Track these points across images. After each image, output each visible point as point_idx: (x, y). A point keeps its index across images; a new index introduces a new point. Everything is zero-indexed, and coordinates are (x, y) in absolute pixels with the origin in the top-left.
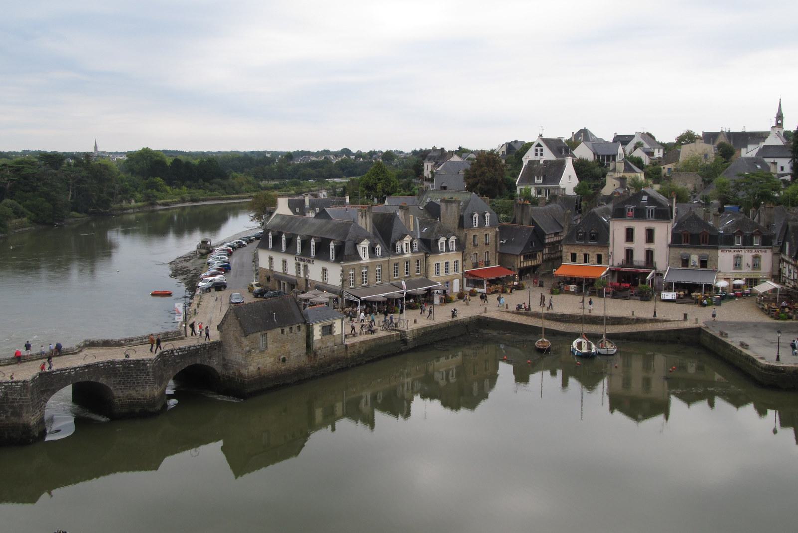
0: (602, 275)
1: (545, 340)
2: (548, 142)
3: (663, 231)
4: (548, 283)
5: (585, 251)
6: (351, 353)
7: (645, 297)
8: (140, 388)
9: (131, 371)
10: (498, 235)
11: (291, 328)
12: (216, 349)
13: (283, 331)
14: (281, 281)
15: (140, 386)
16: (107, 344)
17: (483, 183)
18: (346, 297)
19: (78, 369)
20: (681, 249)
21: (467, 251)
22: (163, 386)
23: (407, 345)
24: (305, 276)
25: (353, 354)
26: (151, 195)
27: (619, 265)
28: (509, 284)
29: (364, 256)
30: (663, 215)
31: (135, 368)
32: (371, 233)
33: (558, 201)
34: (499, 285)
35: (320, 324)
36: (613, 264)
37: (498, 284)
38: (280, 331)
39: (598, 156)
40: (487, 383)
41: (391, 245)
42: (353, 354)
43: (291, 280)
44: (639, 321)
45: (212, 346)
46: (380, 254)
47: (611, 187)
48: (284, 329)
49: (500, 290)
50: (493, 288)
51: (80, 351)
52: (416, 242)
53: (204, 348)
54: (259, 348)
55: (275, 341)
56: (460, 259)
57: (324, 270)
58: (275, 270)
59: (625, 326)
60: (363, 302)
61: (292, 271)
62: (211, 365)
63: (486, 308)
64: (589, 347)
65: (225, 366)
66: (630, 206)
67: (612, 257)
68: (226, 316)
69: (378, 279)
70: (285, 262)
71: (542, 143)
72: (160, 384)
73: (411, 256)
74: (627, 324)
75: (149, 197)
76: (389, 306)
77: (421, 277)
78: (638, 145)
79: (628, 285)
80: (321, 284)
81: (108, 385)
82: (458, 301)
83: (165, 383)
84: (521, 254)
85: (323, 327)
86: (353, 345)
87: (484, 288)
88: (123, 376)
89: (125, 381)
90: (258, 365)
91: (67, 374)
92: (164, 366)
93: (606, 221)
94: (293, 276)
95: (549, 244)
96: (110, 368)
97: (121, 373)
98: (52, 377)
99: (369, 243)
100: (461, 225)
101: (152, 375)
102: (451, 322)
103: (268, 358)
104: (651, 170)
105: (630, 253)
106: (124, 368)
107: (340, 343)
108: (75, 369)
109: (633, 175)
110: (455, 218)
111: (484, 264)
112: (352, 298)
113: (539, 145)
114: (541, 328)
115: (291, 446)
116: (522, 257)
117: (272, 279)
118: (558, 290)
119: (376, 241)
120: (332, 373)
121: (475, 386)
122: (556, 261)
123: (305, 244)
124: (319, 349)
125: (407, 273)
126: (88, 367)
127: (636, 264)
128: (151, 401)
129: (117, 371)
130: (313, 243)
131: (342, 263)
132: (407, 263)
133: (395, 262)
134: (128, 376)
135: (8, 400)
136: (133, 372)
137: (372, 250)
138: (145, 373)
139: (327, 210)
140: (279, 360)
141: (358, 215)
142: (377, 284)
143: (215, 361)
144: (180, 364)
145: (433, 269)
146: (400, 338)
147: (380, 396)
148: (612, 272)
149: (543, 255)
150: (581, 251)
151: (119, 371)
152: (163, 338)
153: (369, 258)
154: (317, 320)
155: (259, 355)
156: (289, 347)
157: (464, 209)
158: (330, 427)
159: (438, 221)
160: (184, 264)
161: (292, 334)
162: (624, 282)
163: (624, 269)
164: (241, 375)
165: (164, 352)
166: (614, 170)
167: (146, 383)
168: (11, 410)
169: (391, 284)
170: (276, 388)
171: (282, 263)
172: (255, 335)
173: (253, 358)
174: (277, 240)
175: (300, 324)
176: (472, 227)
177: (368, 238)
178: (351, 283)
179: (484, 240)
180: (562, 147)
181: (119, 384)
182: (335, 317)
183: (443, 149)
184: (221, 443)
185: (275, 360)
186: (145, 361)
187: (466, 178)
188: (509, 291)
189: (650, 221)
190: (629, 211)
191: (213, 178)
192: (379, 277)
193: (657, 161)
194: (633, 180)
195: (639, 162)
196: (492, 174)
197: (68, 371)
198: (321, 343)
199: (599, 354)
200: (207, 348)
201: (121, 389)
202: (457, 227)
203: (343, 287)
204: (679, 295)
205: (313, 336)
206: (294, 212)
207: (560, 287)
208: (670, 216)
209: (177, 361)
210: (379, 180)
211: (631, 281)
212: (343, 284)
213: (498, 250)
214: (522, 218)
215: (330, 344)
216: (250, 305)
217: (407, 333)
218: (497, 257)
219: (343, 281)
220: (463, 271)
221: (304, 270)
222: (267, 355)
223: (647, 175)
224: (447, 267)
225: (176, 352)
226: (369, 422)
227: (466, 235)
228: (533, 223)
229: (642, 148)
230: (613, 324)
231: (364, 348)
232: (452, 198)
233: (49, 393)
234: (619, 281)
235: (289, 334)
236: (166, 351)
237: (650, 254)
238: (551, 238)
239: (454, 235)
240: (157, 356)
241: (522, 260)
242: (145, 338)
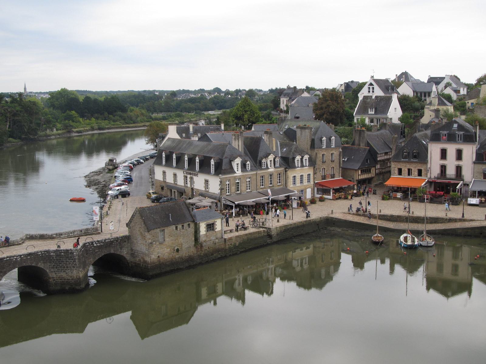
0: (422, 185)
1: (379, 235)
2: (378, 82)
3: (470, 151)
4: (380, 192)
5: (409, 166)
6: (229, 245)
7: (455, 202)
8: (69, 270)
9: (61, 258)
10: (341, 154)
11: (183, 226)
12: (125, 241)
13: (176, 228)
14: (172, 190)
15: (69, 269)
16: (42, 237)
17: (328, 114)
18: (223, 202)
19: (23, 256)
20: (483, 165)
21: (317, 166)
22: (86, 270)
23: (271, 239)
24: (191, 186)
25: (230, 246)
26: (68, 125)
27: (435, 178)
28: (350, 192)
29: (238, 171)
30: (469, 138)
31: (65, 255)
32: (243, 152)
33: (388, 127)
34: (341, 193)
35: (205, 223)
36: (430, 177)
37: (341, 192)
39: (417, 93)
40: (332, 268)
41: (258, 161)
42: (230, 246)
43: (181, 189)
44: (451, 220)
46: (250, 169)
47: (427, 117)
48: (177, 226)
49: (343, 197)
50: (337, 195)
51: (23, 243)
52: (277, 159)
54: (158, 241)
55: (170, 236)
56: (312, 173)
57: (207, 182)
58: (167, 181)
59: (440, 224)
60: (237, 206)
61: (181, 182)
62: (122, 254)
63: (332, 211)
64: (413, 241)
65: (133, 255)
66: (444, 131)
67: (430, 171)
68: (133, 216)
69: (248, 188)
70: (175, 175)
71: (374, 83)
72: (84, 268)
73: (274, 170)
74: (442, 223)
75: (67, 126)
76: (258, 209)
77: (281, 187)
78: (448, 85)
79: (442, 193)
80: (204, 192)
81: (45, 269)
82: (310, 205)
83: (87, 267)
84: (359, 169)
85: (207, 225)
86: (230, 239)
87: (330, 195)
88: (56, 262)
89: (57, 265)
91: (14, 260)
92: (86, 254)
93: (425, 143)
94: (182, 186)
95: (380, 161)
96: (46, 256)
97: (54, 260)
98: (4, 262)
99: (241, 160)
100: (313, 146)
101: (78, 261)
102: (306, 221)
104: (458, 104)
105: (443, 168)
106: (57, 256)
107: (220, 237)
108: (20, 256)
109: (445, 108)
110: (308, 141)
111: (330, 177)
112: (229, 203)
113: (371, 84)
114: (376, 226)
115: (183, 316)
116: (360, 171)
117: (165, 188)
118: (388, 197)
119: (247, 158)
120: (214, 260)
121: (323, 271)
122: (387, 174)
123: (191, 161)
124: (204, 242)
125: (271, 184)
126: (30, 254)
127: (448, 176)
128: (78, 281)
129: (51, 258)
130: (197, 160)
131: (220, 175)
132: (271, 176)
133: (262, 175)
134: (60, 262)
136: (64, 259)
137: (244, 166)
138: (72, 259)
139: (208, 134)
140: (174, 250)
141: (232, 138)
142: (247, 192)
143: (124, 251)
145: (291, 180)
146: (266, 234)
147: (250, 279)
148: (430, 183)
149: (376, 170)
150: (405, 166)
151: (53, 258)
152: (84, 233)
153: (242, 172)
154: (203, 220)
156: (181, 240)
157: (315, 134)
158: (212, 302)
159: (295, 143)
160: (96, 177)
161: (184, 230)
162: (439, 191)
163: (439, 181)
164: (145, 262)
165: (86, 243)
166: (430, 104)
167: (74, 267)
169: (259, 192)
170: (172, 272)
171: (173, 175)
172: (156, 231)
173: (154, 249)
174: (169, 158)
175: (190, 223)
176: (321, 148)
177: (240, 156)
178: (227, 191)
179: (331, 158)
180: (389, 86)
181: (53, 268)
182: (216, 217)
183: (295, 88)
184: (129, 313)
185: (170, 250)
186: (72, 250)
187: (315, 110)
188: (350, 197)
189: (459, 143)
190: (443, 136)
191: (116, 111)
192: (249, 186)
193: (462, 97)
194: (445, 112)
195: (449, 98)
196: (336, 107)
197: (15, 257)
198: (206, 237)
199: (421, 246)
200: (119, 241)
201: (54, 272)
202: (309, 148)
203: (221, 194)
204: (481, 200)
205: (200, 232)
206: (181, 136)
207: (390, 194)
208: (474, 140)
209: (96, 251)
210: (246, 111)
211: (445, 189)
212: (221, 192)
213: (341, 166)
214: (359, 141)
215: (213, 238)
216: (151, 207)
217: (272, 230)
218: (341, 172)
219: (221, 189)
220: (314, 182)
221: (191, 181)
222: (165, 247)
223: (455, 108)
224: (301, 179)
225: (96, 244)
226: (241, 298)
227: (316, 153)
228: (368, 144)
229: (451, 87)
230: (431, 223)
231: (239, 241)
232: (305, 125)
234: (435, 190)
236: (88, 243)
237: (459, 169)
238: (382, 156)
239: (307, 154)
240: (81, 247)
241: (360, 173)
242: (71, 233)
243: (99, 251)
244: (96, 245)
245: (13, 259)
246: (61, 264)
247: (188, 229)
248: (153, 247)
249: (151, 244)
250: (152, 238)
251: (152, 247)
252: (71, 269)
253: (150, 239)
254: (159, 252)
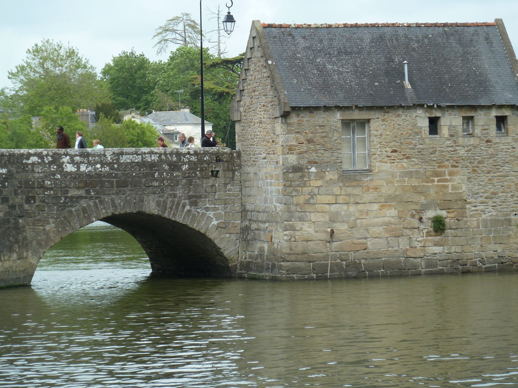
13: (434, 123)
38: (426, 123)
45: (201, 161)
53: (170, 164)
54: (337, 164)
90: (332, 221)
103: (376, 207)
143: (211, 214)
144: (84, 203)
155: (336, 190)
156: (459, 183)
172: (320, 118)
173: (312, 195)
175: (506, 112)
200: (185, 167)
235: (461, 140)
244: (74, 169)
247: (498, 140)
248: (306, 190)
249: (299, 174)
251: (305, 186)
254: (337, 213)
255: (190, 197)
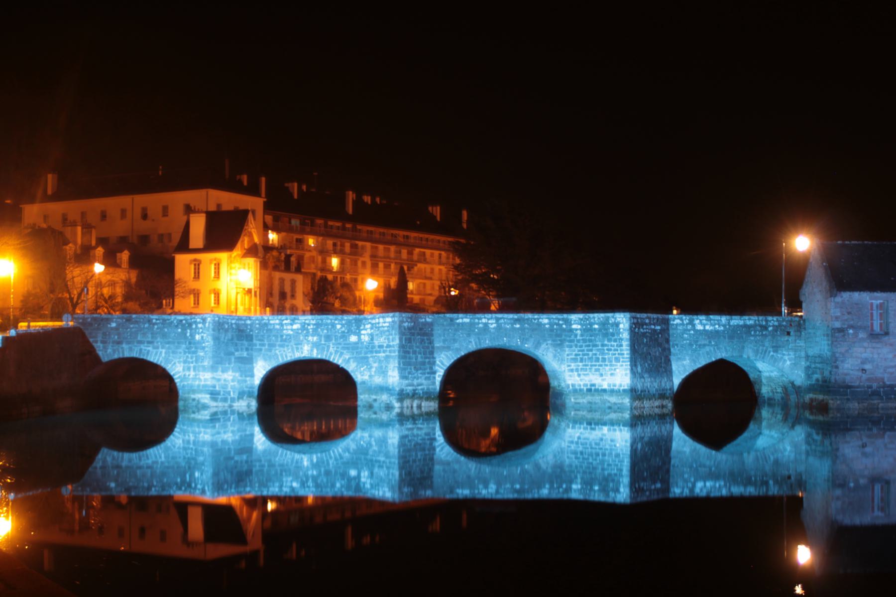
8: (607, 368)
12: (789, 333)
19: (502, 321)
88: (581, 346)
90: (863, 363)
91: (481, 325)
97: (578, 341)
129: (573, 337)
134: (589, 346)
135: (373, 347)
138: (615, 341)
143: (786, 358)
144: (707, 349)
155: (865, 344)
167: (617, 360)
168: (375, 365)
181: (575, 360)
200: (770, 329)
201: (577, 370)
225: (701, 323)
233: (449, 353)
243: (710, 345)
245: (479, 323)
246: (591, 350)
250: (846, 317)
252: (611, 365)
253: (837, 318)
255: (773, 347)
